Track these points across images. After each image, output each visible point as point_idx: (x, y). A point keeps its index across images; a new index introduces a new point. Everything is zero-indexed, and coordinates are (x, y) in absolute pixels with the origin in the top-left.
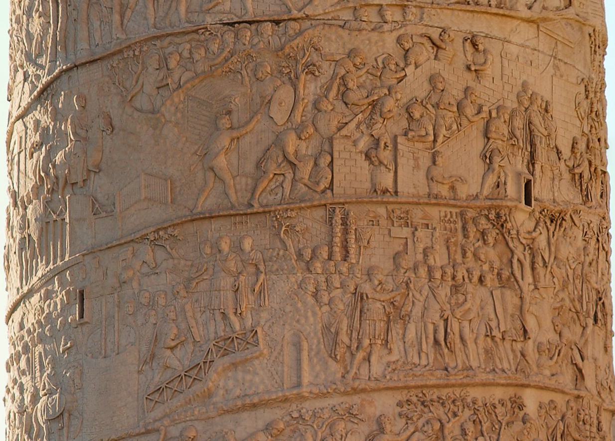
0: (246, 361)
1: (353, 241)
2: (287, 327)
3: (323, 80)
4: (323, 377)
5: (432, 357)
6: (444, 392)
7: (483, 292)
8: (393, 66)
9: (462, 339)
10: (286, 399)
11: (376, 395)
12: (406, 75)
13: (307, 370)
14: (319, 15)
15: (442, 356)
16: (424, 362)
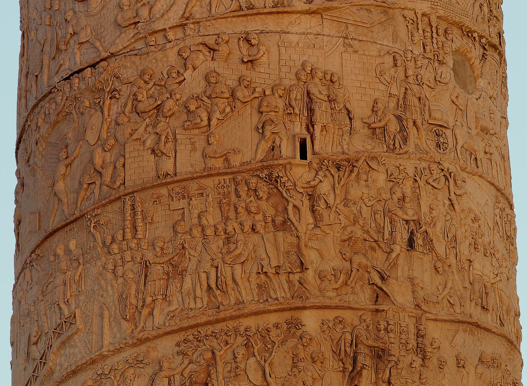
0: (70, 337)
1: (140, 221)
2: (96, 302)
3: (122, 100)
4: (118, 336)
5: (206, 299)
6: (218, 327)
7: (255, 238)
8: (175, 74)
9: (234, 280)
10: (93, 361)
11: (158, 341)
12: (185, 79)
13: (108, 334)
14: (121, 50)
15: (215, 297)
16: (199, 305)
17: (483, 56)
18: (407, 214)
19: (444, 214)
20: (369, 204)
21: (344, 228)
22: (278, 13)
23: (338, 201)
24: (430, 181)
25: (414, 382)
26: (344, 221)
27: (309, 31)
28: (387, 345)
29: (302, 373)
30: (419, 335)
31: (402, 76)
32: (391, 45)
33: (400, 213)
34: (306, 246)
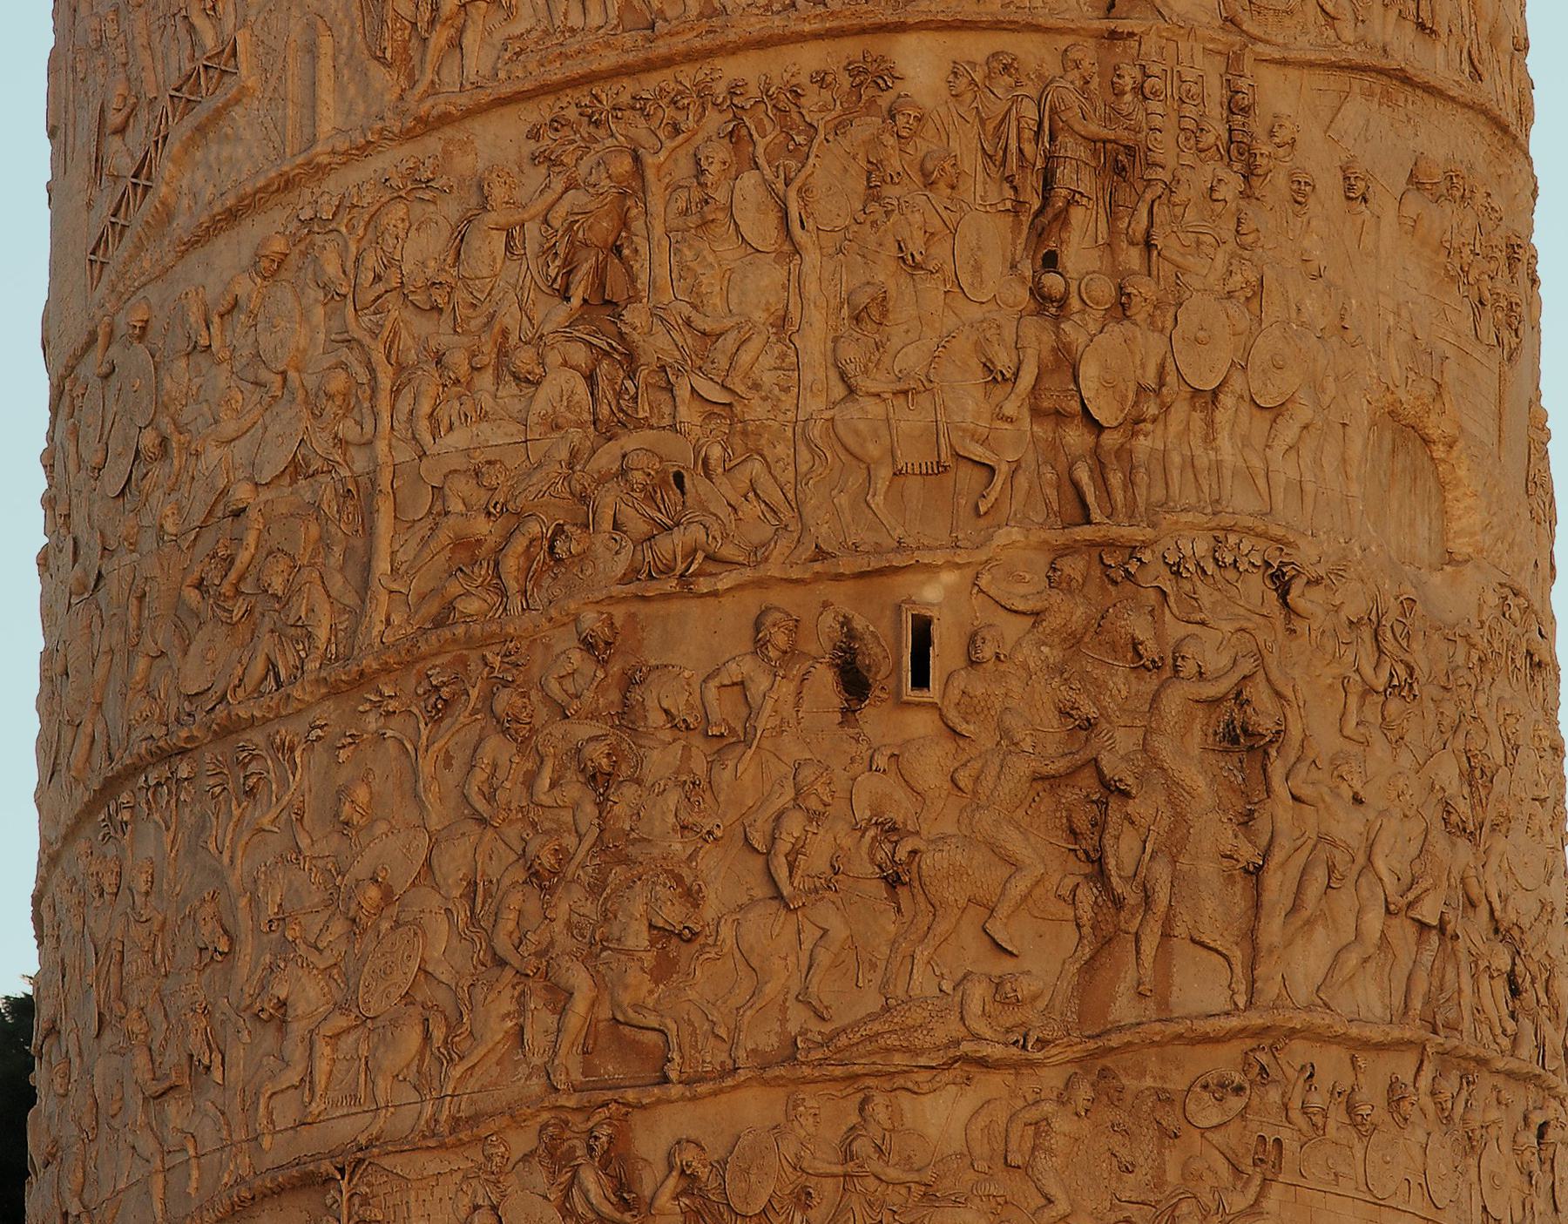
0: (219, 113)
2: (295, 12)
4: (361, 108)
10: (287, 182)
11: (476, 125)
13: (331, 102)
16: (595, 19)
25: (1220, 243)
28: (1142, 136)
29: (894, 217)
30: (1235, 107)
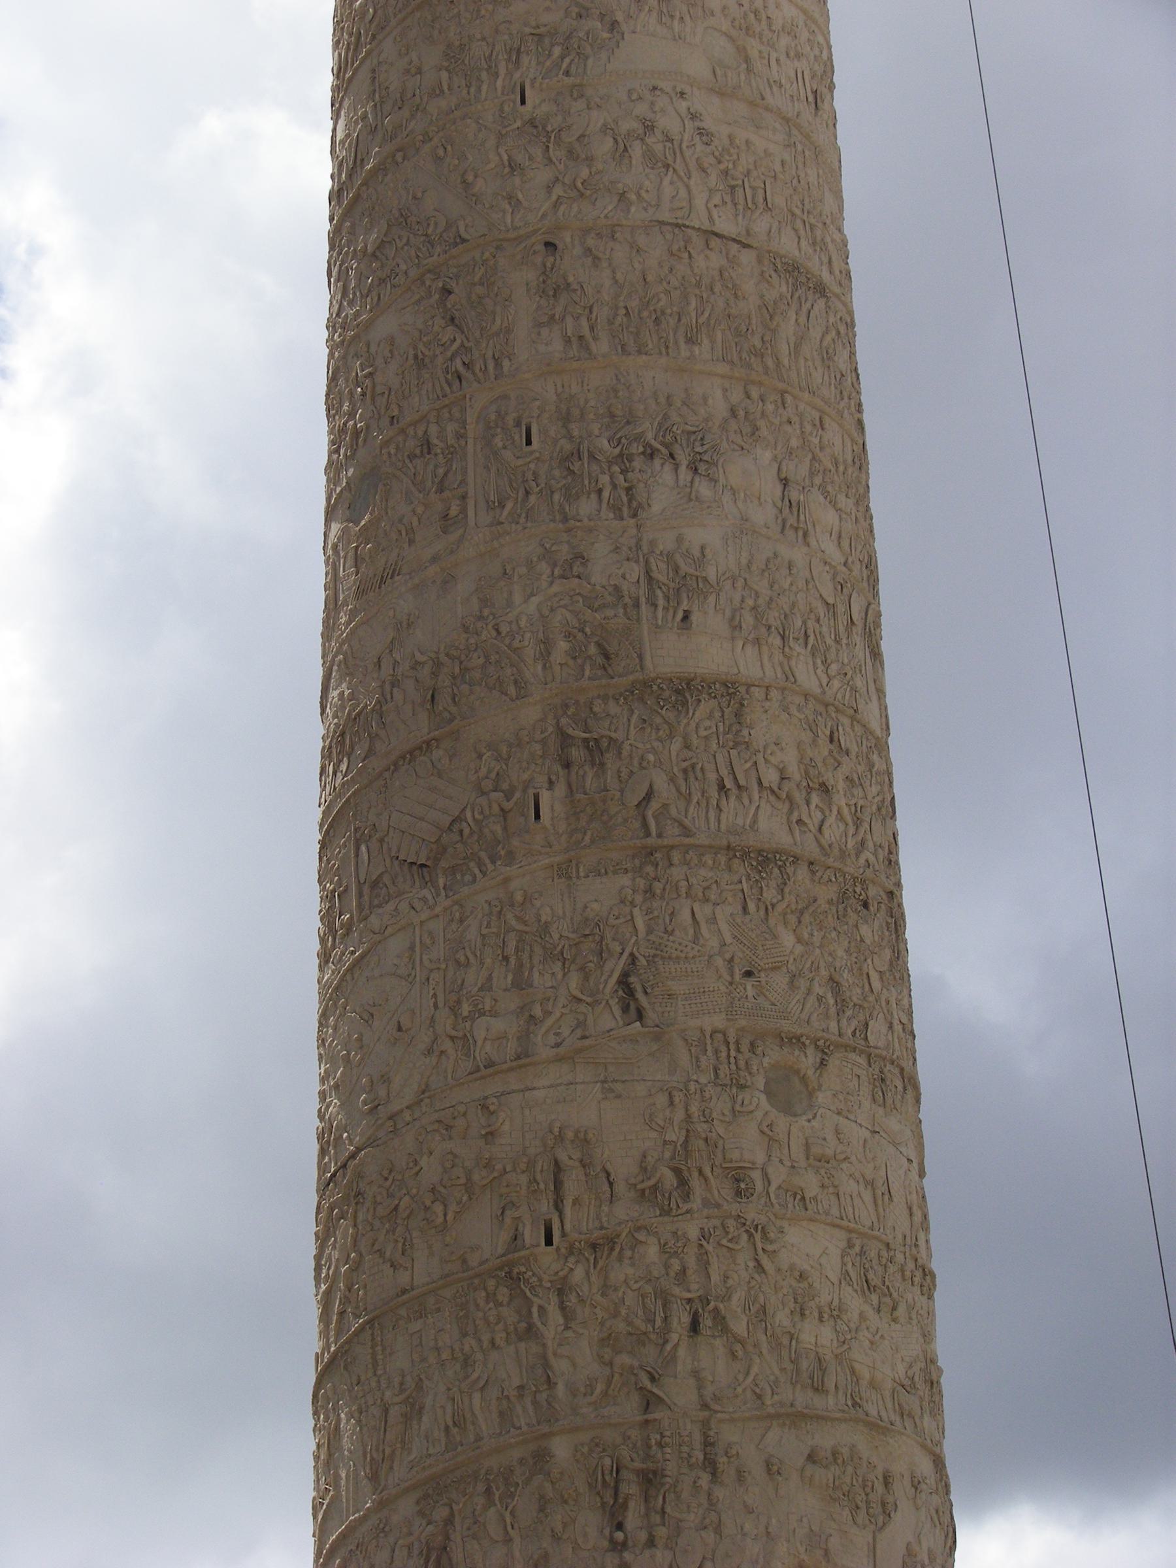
9: (473, 1414)
17: (822, 1063)
18: (689, 1291)
19: (747, 1280)
20: (636, 1286)
21: (602, 1324)
22: (520, 1067)
23: (594, 1290)
24: (724, 1242)
25: (700, 1505)
26: (600, 1314)
27: (559, 1081)
28: (660, 1465)
30: (707, 1444)
31: (680, 1115)
32: (667, 1078)
33: (677, 1290)
34: (555, 1354)
